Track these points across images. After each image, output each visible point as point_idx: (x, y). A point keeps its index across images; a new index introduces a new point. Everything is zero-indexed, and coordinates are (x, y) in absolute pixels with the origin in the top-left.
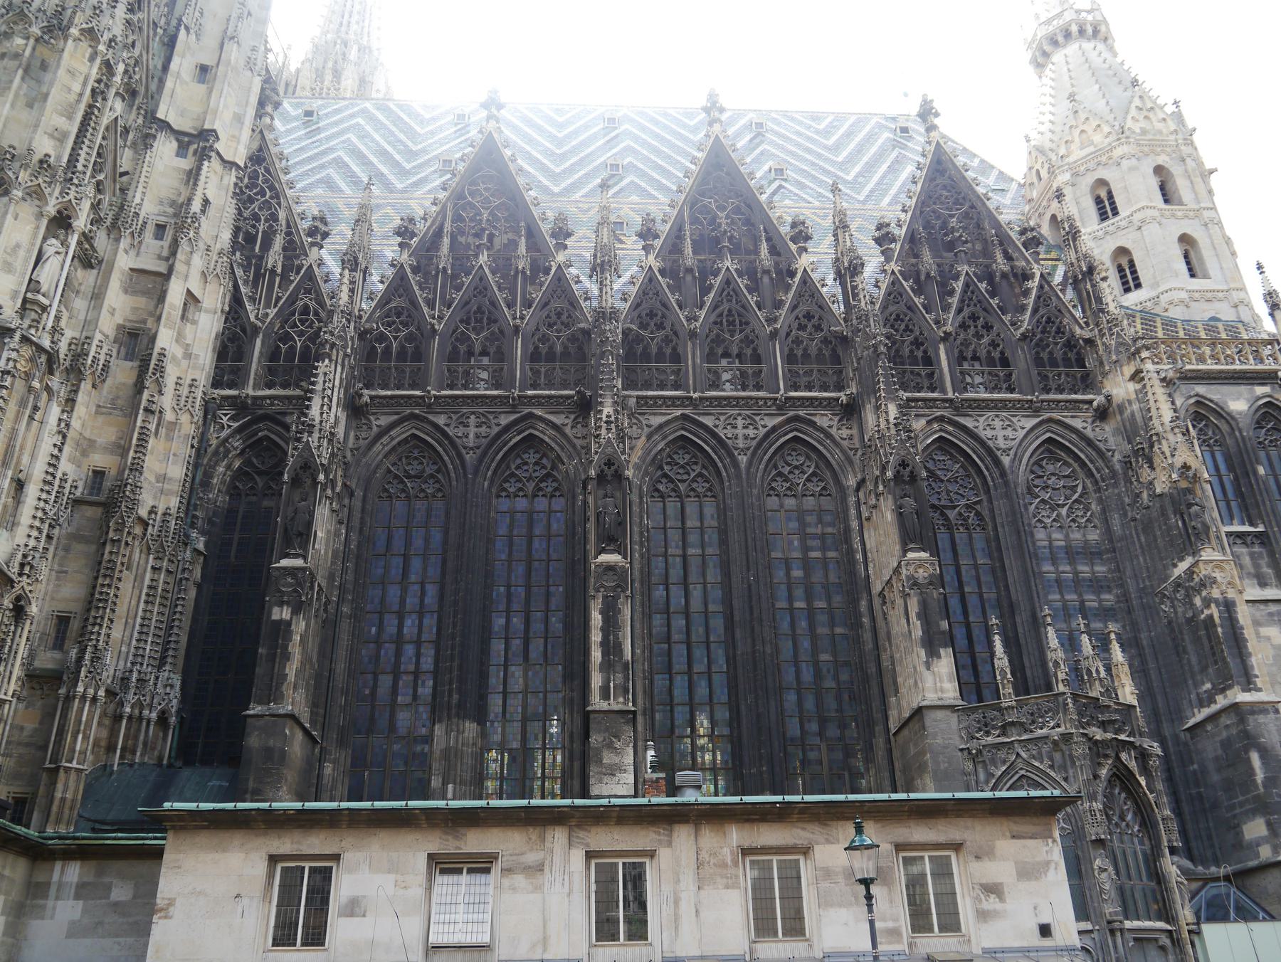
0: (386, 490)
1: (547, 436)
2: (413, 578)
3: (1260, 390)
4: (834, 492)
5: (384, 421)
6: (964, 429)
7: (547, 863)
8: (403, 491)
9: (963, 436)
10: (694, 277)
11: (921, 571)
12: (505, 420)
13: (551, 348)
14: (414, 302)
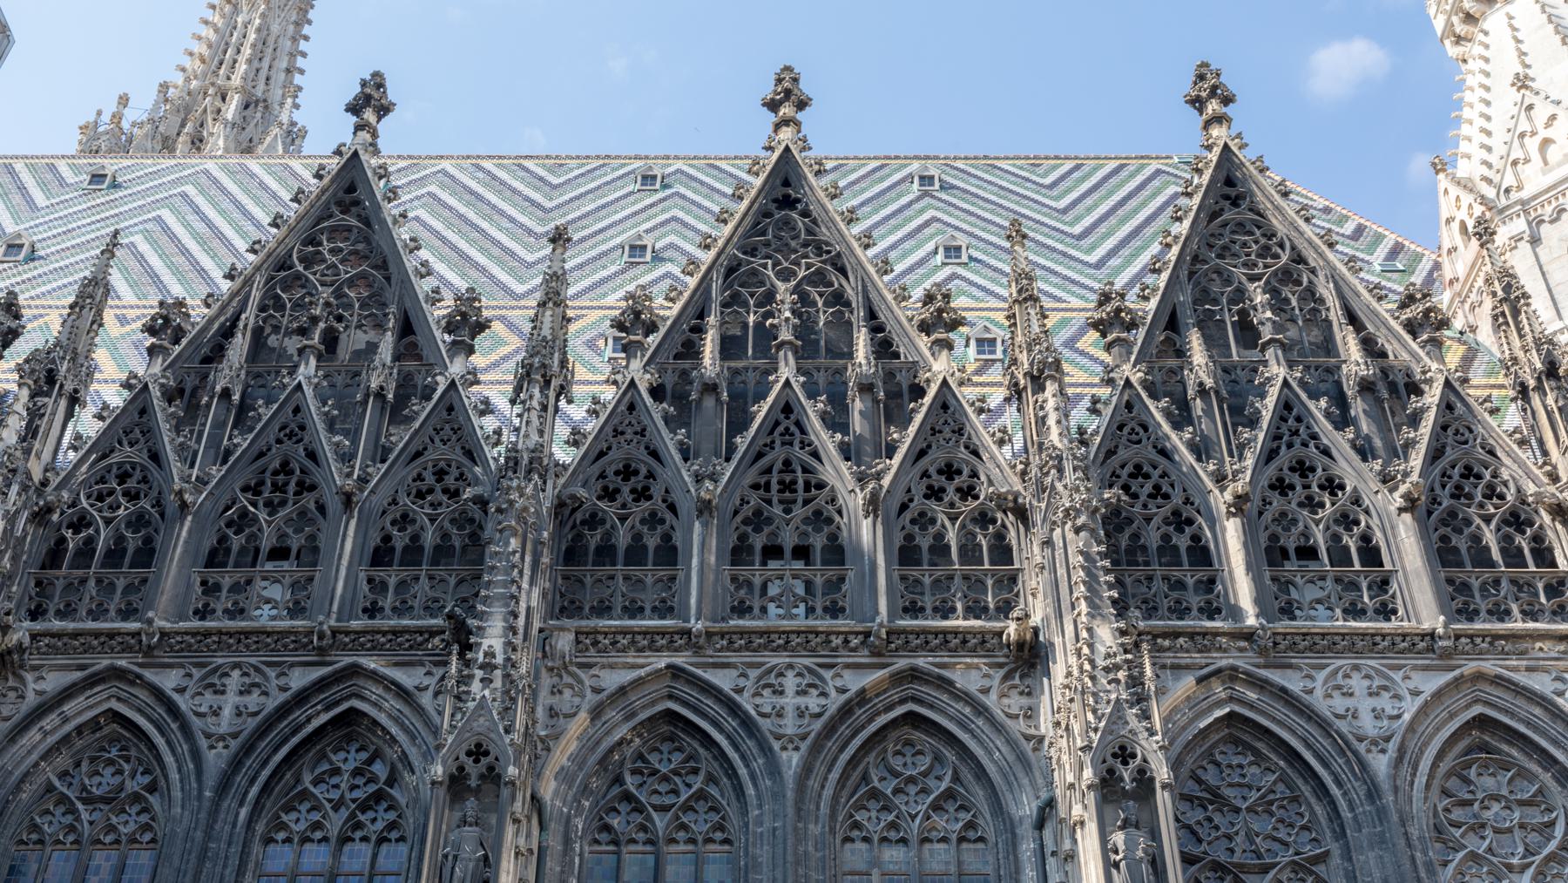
0: (35, 828)
1: (381, 708)
4: (991, 835)
5: (54, 682)
6: (1283, 695)
8: (71, 829)
9: (1280, 711)
10: (718, 400)
12: (299, 679)
13: (415, 538)
14: (155, 457)
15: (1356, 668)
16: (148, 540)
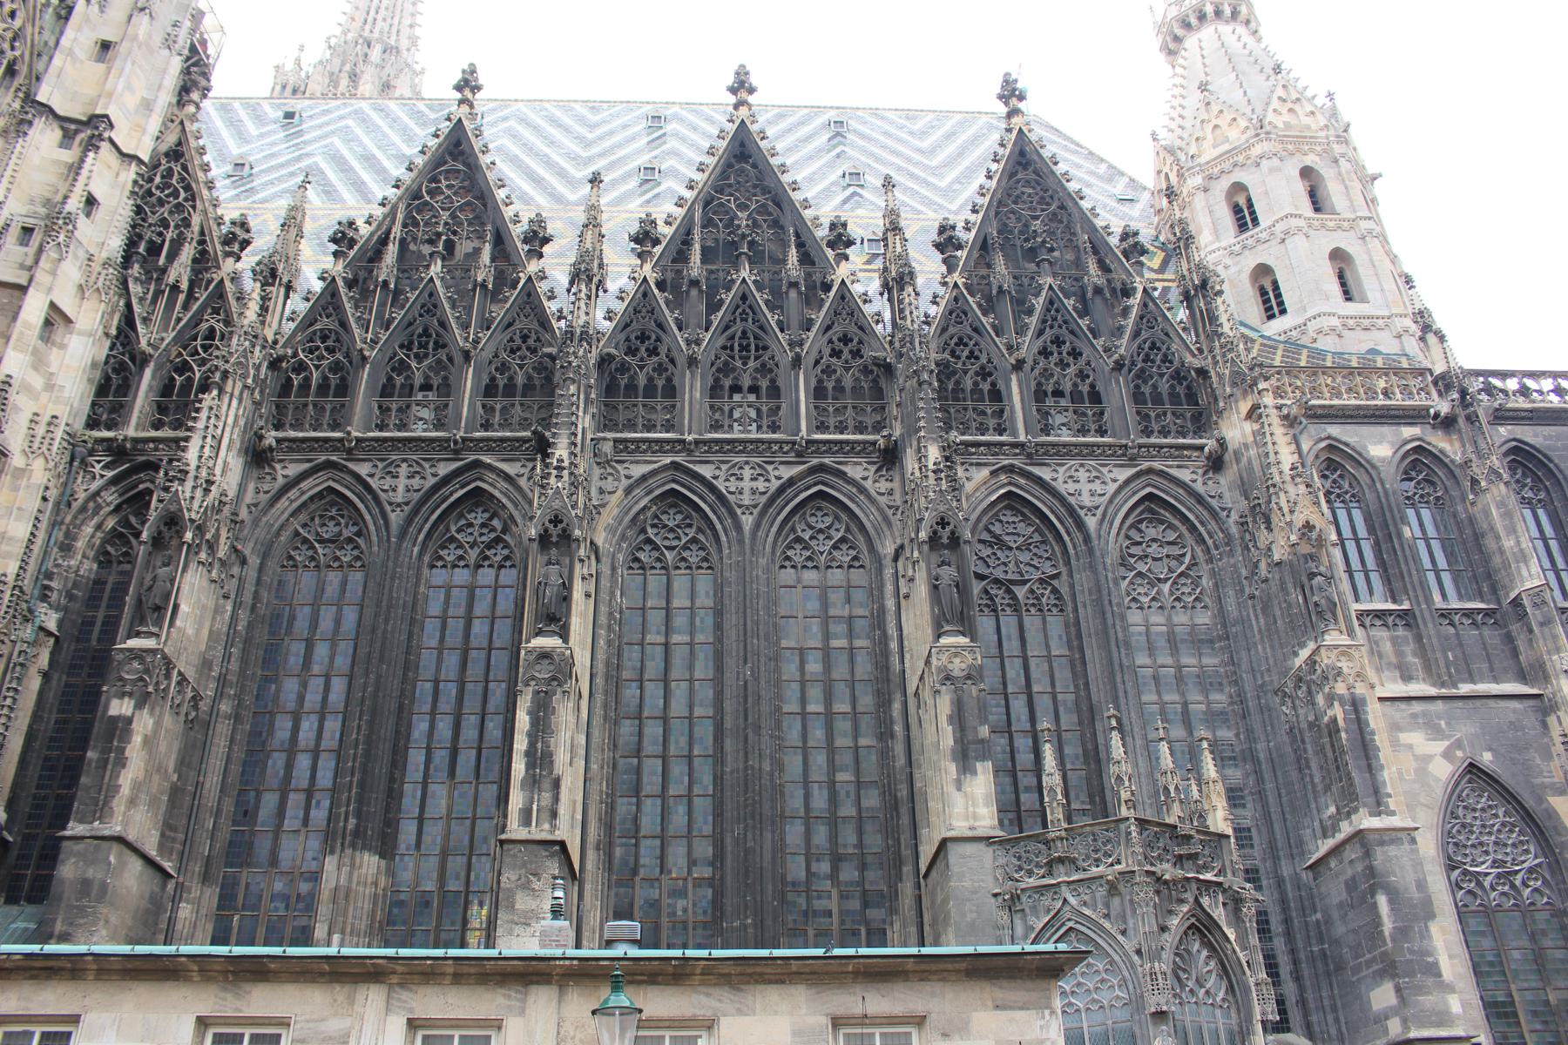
0: (291, 558)
1: (497, 489)
2: (316, 669)
3: (1408, 432)
4: (867, 563)
5: (294, 470)
6: (1039, 481)
7: (354, 1033)
8: (312, 558)
9: (1038, 490)
10: (701, 291)
11: (957, 661)
12: (444, 469)
13: (511, 379)
14: (344, 324)
15: (1082, 465)
16: (343, 379)
